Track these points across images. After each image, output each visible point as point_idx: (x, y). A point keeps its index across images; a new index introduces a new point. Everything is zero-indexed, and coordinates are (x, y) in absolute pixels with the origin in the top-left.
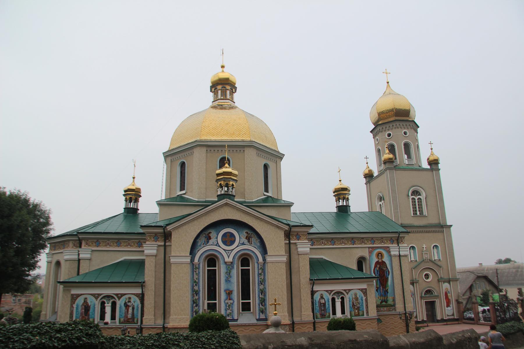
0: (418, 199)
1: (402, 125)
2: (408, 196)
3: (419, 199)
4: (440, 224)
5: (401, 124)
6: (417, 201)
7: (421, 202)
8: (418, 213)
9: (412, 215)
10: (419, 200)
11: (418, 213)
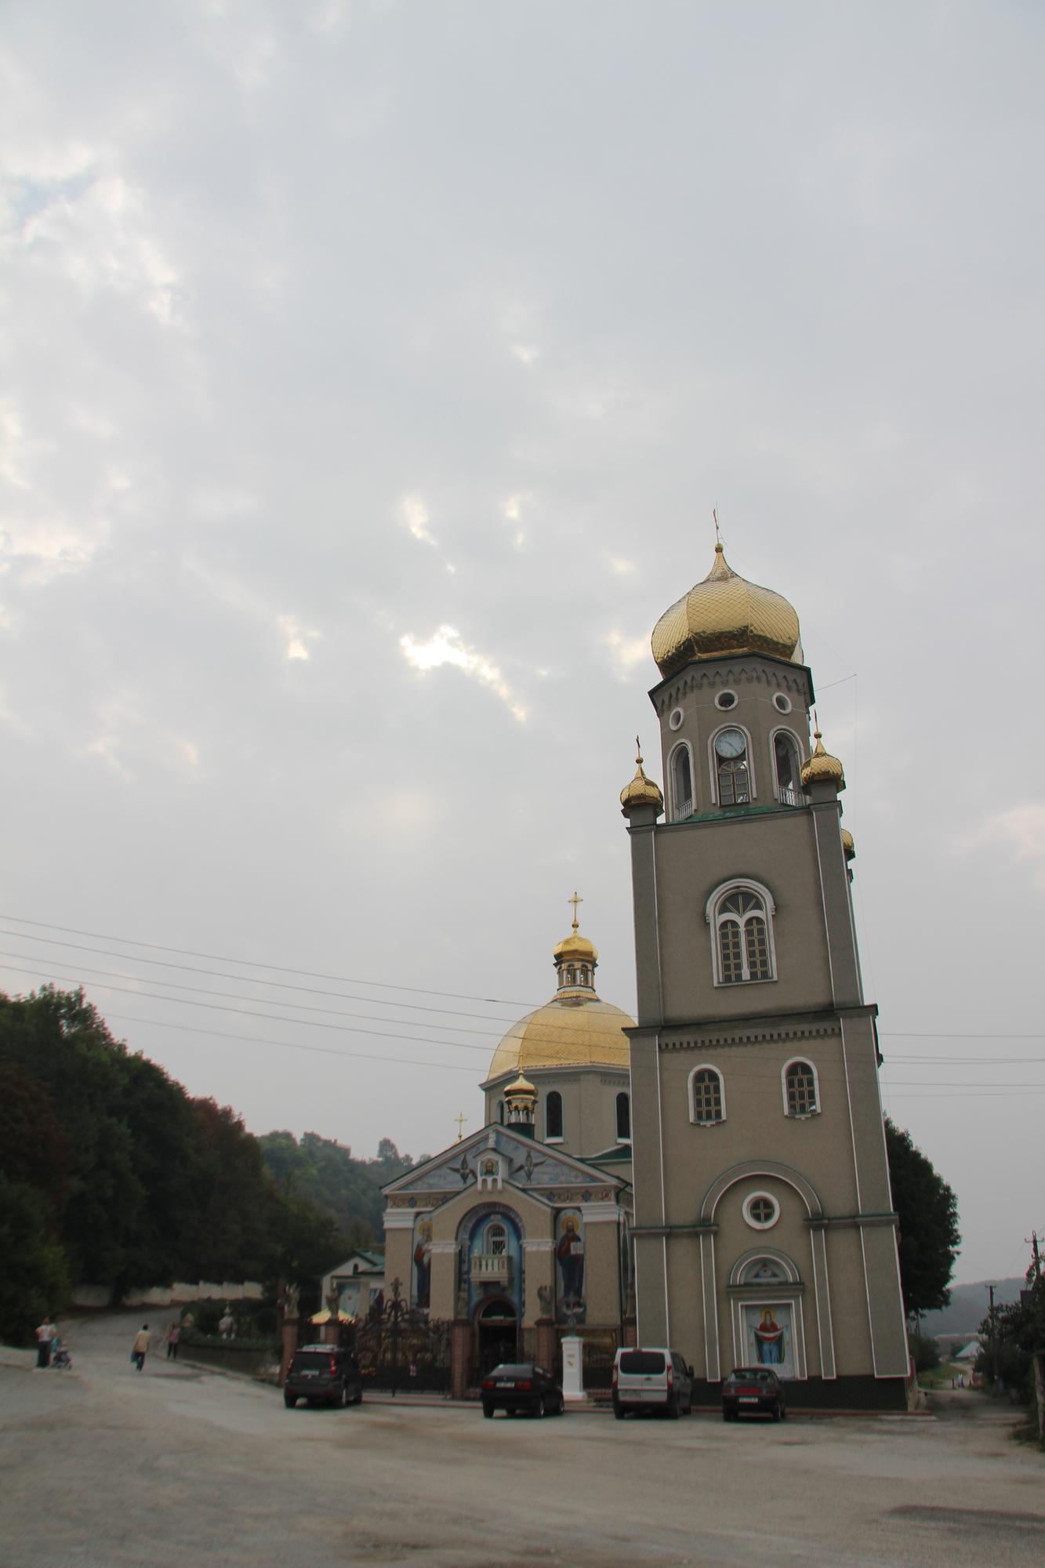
0: (749, 922)
1: (761, 670)
2: (703, 915)
3: (754, 922)
4: (831, 1004)
5: (723, 671)
6: (742, 929)
7: (761, 931)
8: (746, 973)
9: (716, 984)
10: (755, 926)
11: (746, 973)
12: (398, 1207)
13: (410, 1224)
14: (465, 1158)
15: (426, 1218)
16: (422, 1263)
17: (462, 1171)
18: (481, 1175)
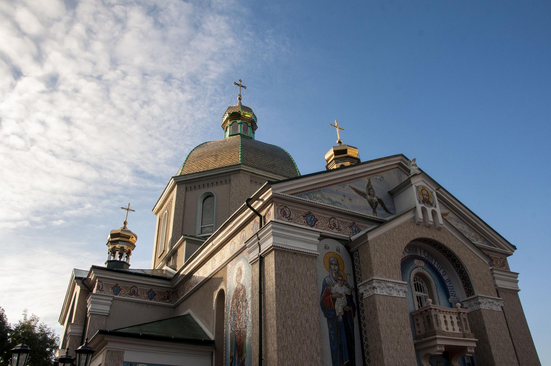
12: (290, 219)
13: (312, 248)
14: (369, 183)
15: (334, 245)
16: (334, 311)
17: (369, 197)
18: (420, 202)
